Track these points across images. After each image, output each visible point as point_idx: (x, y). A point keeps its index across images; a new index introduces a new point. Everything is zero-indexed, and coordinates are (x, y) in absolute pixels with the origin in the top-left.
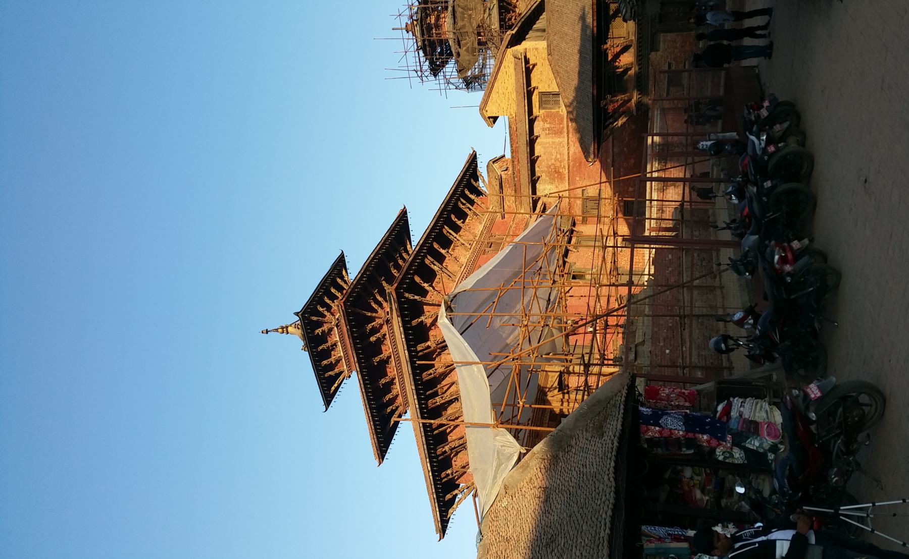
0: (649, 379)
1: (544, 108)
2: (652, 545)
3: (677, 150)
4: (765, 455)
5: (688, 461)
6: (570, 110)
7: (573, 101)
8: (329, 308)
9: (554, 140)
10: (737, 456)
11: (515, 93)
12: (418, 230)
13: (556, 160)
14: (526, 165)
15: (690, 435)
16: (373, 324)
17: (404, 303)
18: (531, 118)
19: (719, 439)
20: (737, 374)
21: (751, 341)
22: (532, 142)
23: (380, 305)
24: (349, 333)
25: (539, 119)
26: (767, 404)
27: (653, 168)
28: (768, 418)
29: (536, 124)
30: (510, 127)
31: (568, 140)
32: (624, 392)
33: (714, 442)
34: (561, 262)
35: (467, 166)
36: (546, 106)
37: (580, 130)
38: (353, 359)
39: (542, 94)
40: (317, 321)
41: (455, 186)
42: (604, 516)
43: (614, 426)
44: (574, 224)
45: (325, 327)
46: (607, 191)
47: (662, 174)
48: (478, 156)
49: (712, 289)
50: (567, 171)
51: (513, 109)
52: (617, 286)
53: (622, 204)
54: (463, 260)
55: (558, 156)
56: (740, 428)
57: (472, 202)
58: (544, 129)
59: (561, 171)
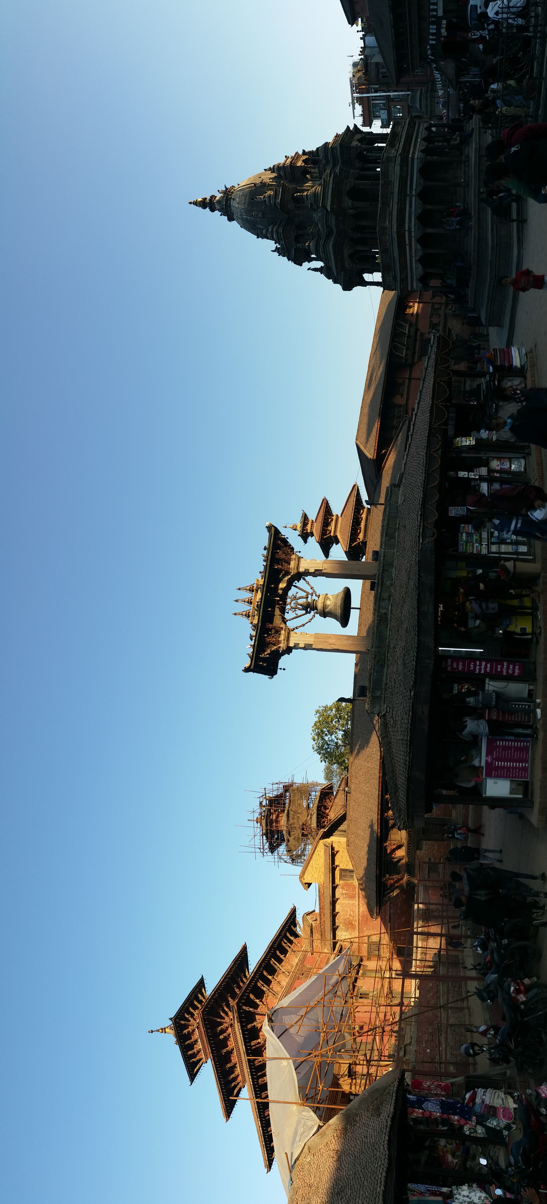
0: (414, 1072)
1: (343, 880)
2: (416, 1198)
3: (435, 914)
4: (500, 1132)
5: (443, 1135)
6: (361, 882)
7: (363, 876)
8: (192, 1015)
9: (349, 902)
10: (480, 1131)
11: (323, 868)
12: (254, 961)
13: (350, 915)
14: (329, 918)
15: (445, 1116)
16: (221, 1027)
17: (242, 1013)
18: (334, 885)
19: (466, 1119)
20: (480, 1072)
21: (493, 1048)
22: (334, 902)
23: (227, 1014)
24: (206, 1033)
25: (339, 887)
26: (503, 1093)
27: (418, 926)
28: (503, 1104)
29: (337, 890)
30: (319, 891)
31: (359, 902)
32: (396, 1084)
33: (463, 1122)
34: (351, 987)
35: (289, 917)
36: (344, 878)
37: (367, 897)
38: (209, 1050)
39: (342, 870)
40: (185, 1024)
41: (280, 930)
42: (380, 1176)
43: (388, 1109)
44: (362, 960)
45: (190, 1029)
46: (386, 939)
47: (426, 930)
48: (297, 910)
49: (461, 1009)
50: (357, 923)
51: (322, 879)
52: (392, 1006)
53: (396, 948)
54: (284, 983)
55: (352, 913)
56: (482, 1112)
57: (291, 942)
58: (342, 894)
59: (353, 923)
